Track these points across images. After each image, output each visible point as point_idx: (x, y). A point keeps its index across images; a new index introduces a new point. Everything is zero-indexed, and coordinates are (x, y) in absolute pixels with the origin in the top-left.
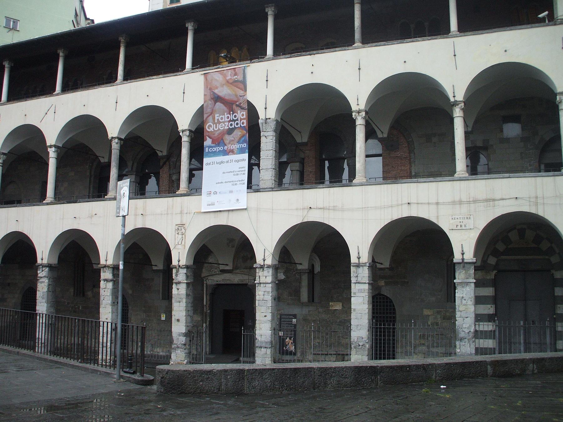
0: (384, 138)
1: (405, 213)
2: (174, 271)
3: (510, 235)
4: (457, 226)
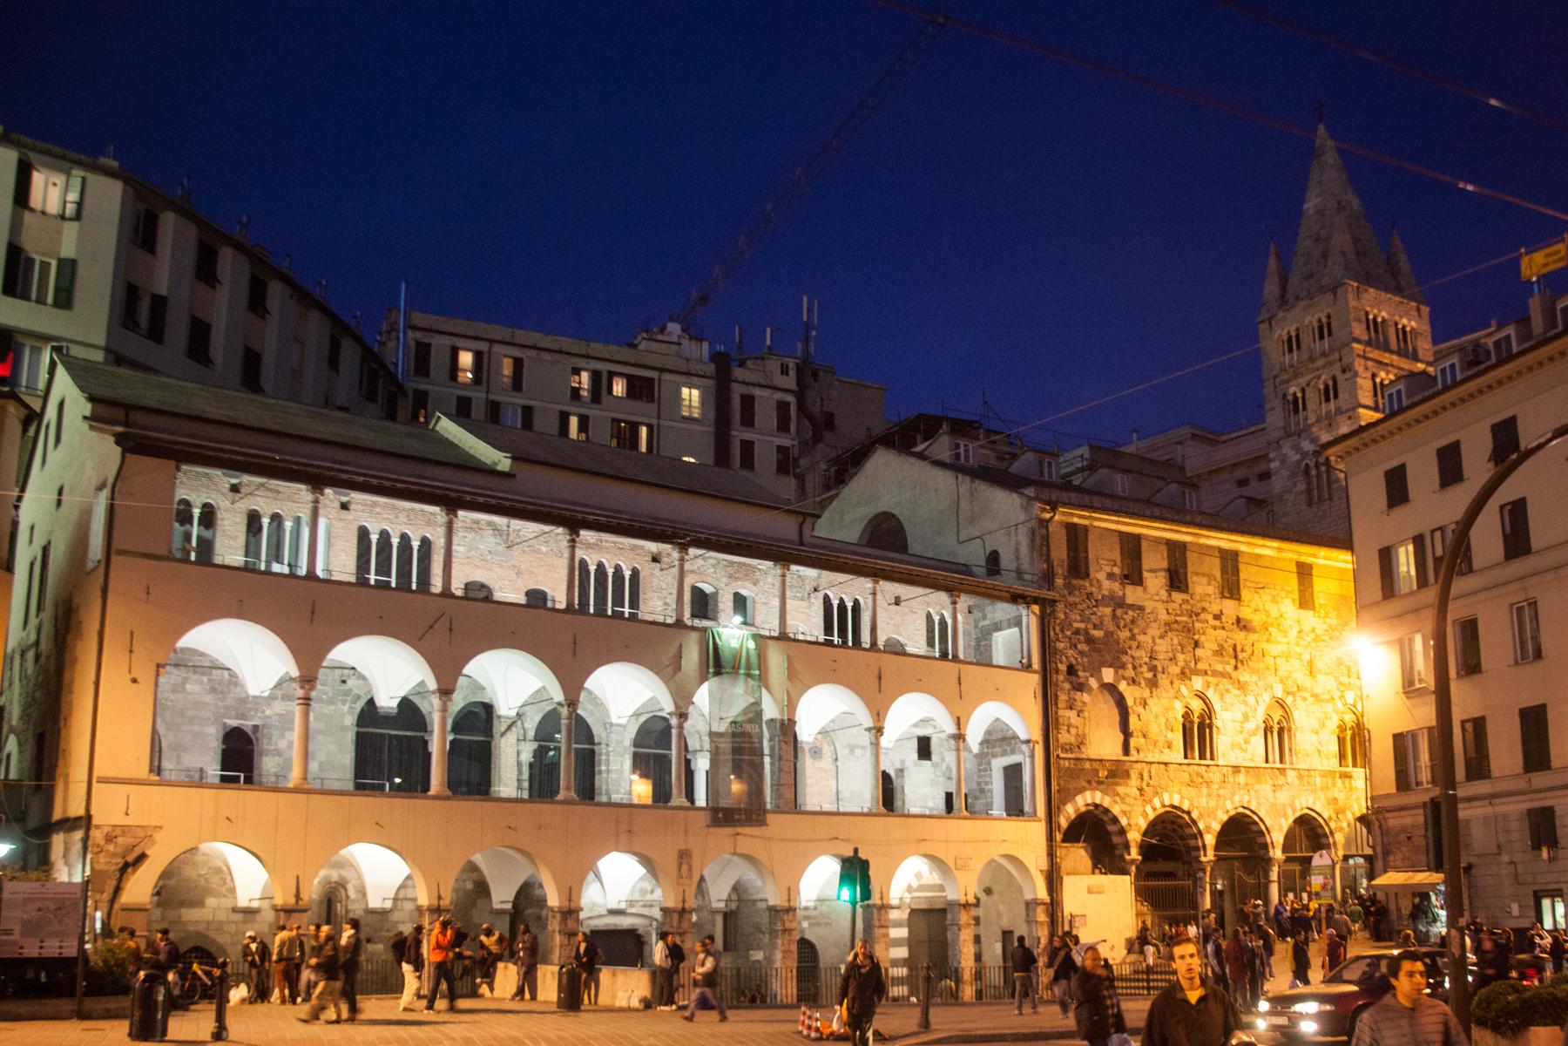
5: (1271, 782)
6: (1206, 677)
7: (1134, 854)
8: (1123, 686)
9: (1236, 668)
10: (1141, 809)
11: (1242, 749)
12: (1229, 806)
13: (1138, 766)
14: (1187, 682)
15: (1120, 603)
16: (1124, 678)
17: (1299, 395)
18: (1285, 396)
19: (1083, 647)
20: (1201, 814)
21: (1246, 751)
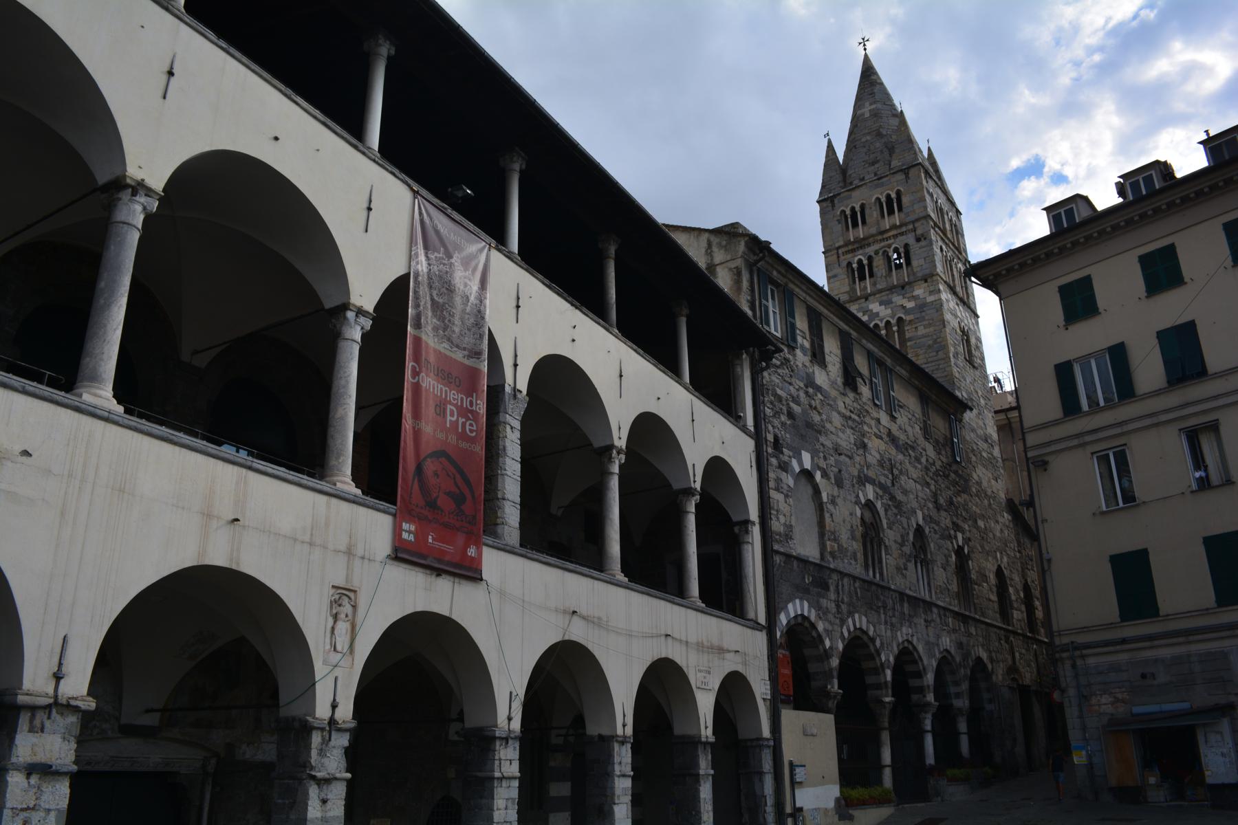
2: (316, 739)
4: (702, 682)
5: (923, 615)
7: (834, 687)
8: (818, 476)
9: (893, 485)
10: (840, 630)
11: (902, 574)
12: (900, 640)
13: (835, 577)
14: (863, 488)
15: (810, 382)
16: (819, 468)
17: (865, 262)
18: (850, 264)
19: (783, 418)
20: (882, 644)
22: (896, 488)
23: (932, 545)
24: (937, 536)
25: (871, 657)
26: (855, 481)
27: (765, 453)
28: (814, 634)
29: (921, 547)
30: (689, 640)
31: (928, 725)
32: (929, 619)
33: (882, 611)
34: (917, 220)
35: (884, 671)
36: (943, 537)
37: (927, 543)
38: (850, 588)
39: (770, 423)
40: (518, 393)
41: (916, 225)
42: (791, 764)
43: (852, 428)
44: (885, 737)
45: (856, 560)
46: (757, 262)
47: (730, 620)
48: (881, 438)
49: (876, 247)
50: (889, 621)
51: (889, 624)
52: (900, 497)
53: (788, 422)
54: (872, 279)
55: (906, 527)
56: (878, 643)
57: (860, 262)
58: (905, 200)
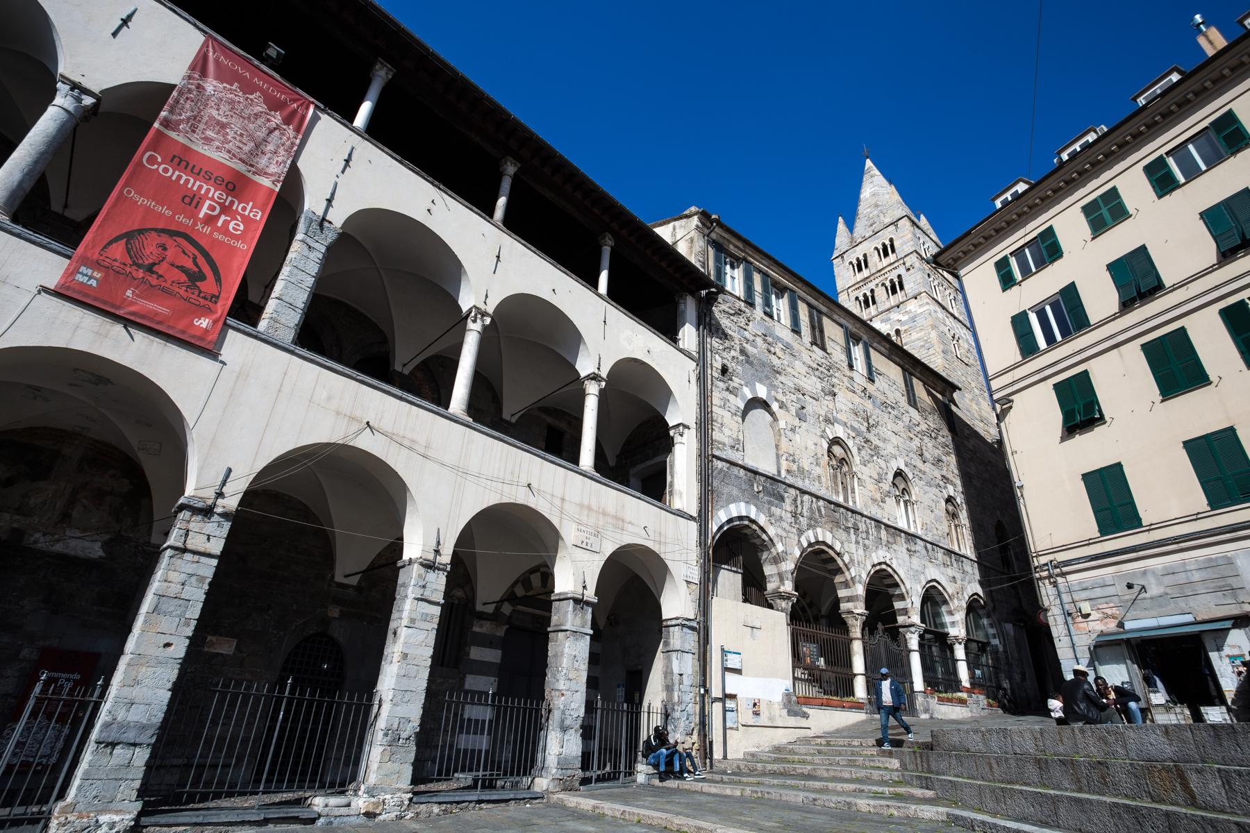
0: (404, 375)
1: (521, 497)
3: (532, 577)
4: (583, 542)
5: (904, 544)
6: (846, 429)
7: (788, 587)
8: (775, 406)
10: (796, 538)
11: (878, 505)
13: (792, 491)
16: (776, 400)
17: (869, 294)
18: (857, 298)
21: (883, 509)
22: (872, 434)
23: (917, 488)
24: (923, 483)
25: (839, 571)
26: (821, 419)
27: (709, 377)
28: (764, 537)
29: (904, 489)
30: (567, 498)
31: (913, 642)
32: (913, 549)
33: (852, 531)
34: (906, 256)
35: (854, 584)
36: (929, 484)
37: (911, 487)
38: (811, 505)
39: (717, 353)
40: (326, 224)
41: (905, 259)
42: (724, 652)
43: (820, 378)
44: (857, 648)
45: (820, 483)
46: (710, 233)
47: (639, 498)
48: (854, 392)
49: (877, 281)
50: (861, 541)
51: (861, 544)
52: (876, 441)
53: (741, 358)
54: (875, 306)
55: (885, 468)
56: (846, 558)
57: (865, 295)
58: (896, 244)
